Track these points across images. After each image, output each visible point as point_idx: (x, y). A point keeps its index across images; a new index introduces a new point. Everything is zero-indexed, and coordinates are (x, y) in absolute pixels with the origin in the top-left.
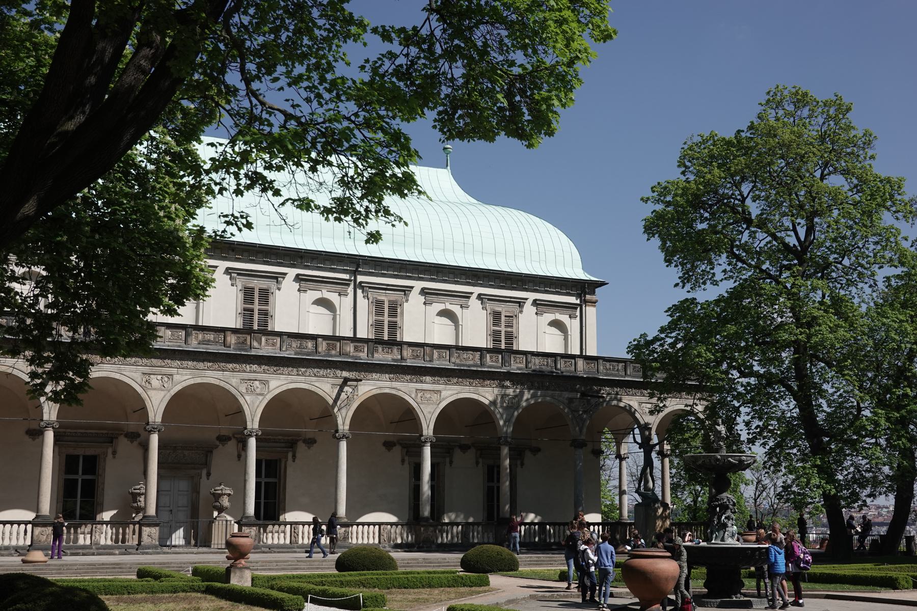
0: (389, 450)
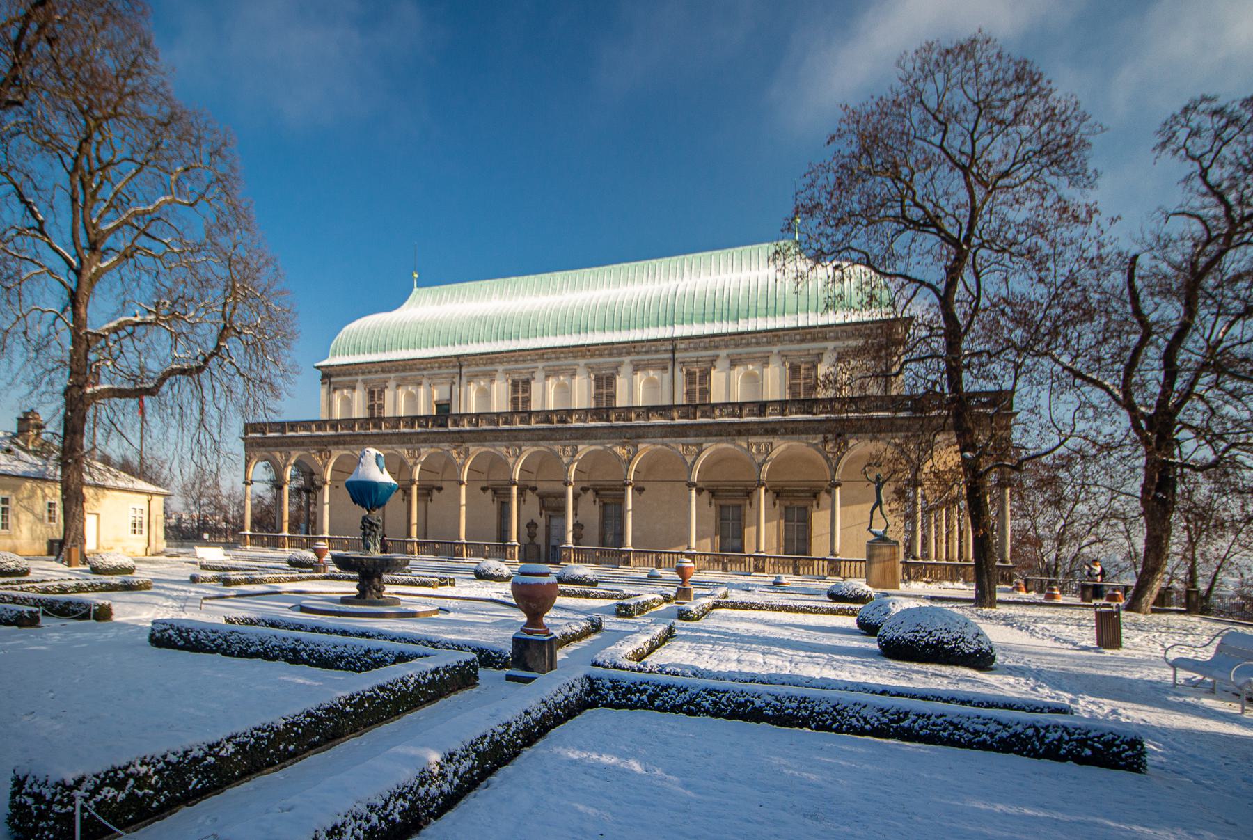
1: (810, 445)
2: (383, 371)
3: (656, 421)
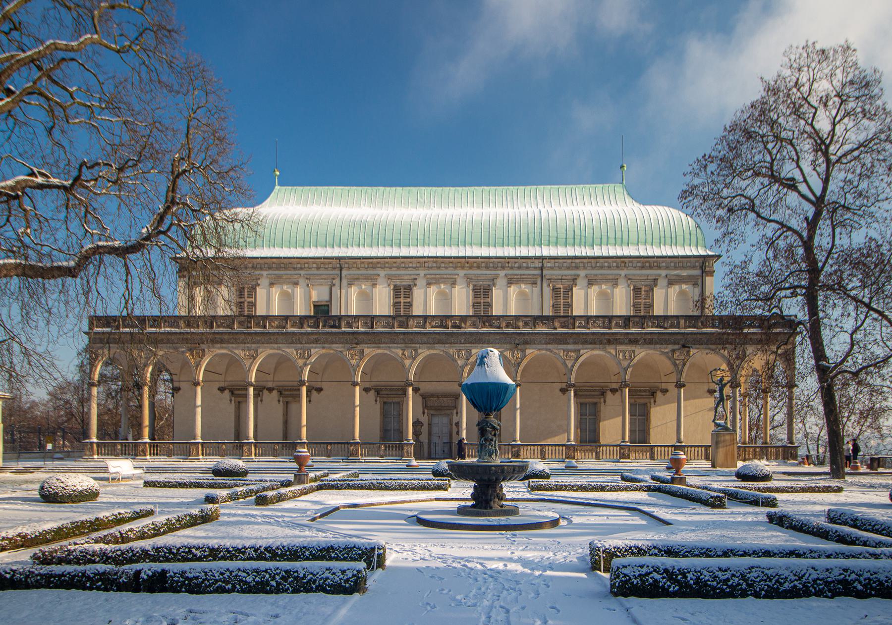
3: (540, 329)
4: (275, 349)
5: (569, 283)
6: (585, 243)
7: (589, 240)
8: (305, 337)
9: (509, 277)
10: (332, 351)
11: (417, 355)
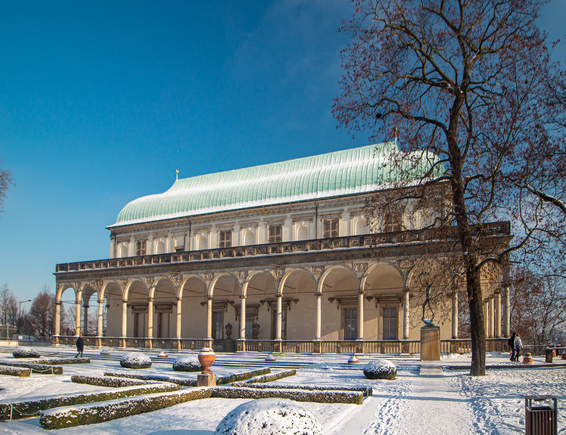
0: (331, 302)
1: (391, 264)
2: (146, 229)
3: (296, 251)
4: (136, 278)
5: (335, 217)
6: (349, 185)
7: (352, 182)
8: (151, 269)
9: (293, 217)
10: (165, 278)
11: (214, 277)
